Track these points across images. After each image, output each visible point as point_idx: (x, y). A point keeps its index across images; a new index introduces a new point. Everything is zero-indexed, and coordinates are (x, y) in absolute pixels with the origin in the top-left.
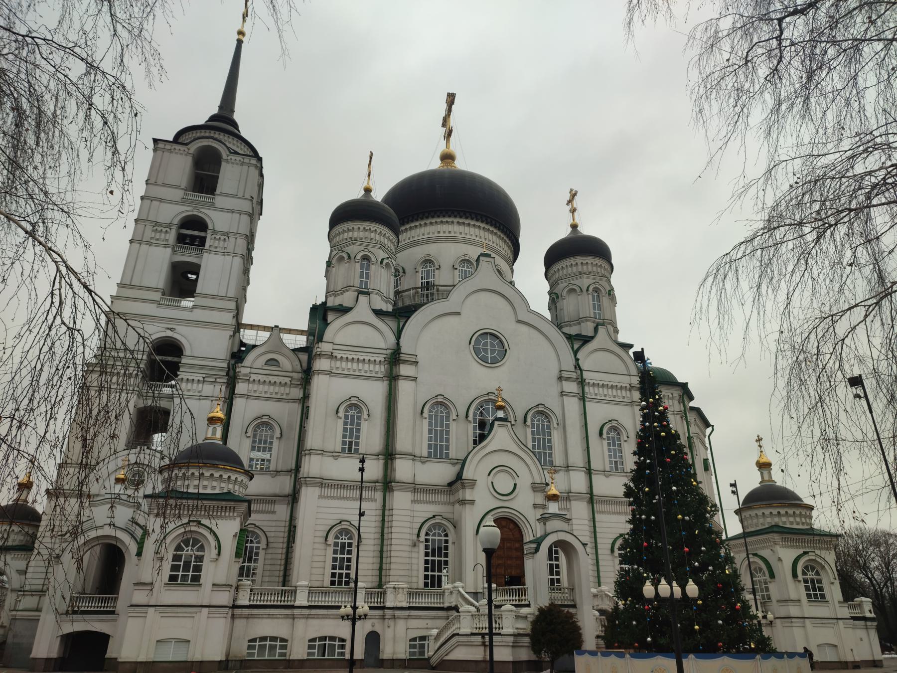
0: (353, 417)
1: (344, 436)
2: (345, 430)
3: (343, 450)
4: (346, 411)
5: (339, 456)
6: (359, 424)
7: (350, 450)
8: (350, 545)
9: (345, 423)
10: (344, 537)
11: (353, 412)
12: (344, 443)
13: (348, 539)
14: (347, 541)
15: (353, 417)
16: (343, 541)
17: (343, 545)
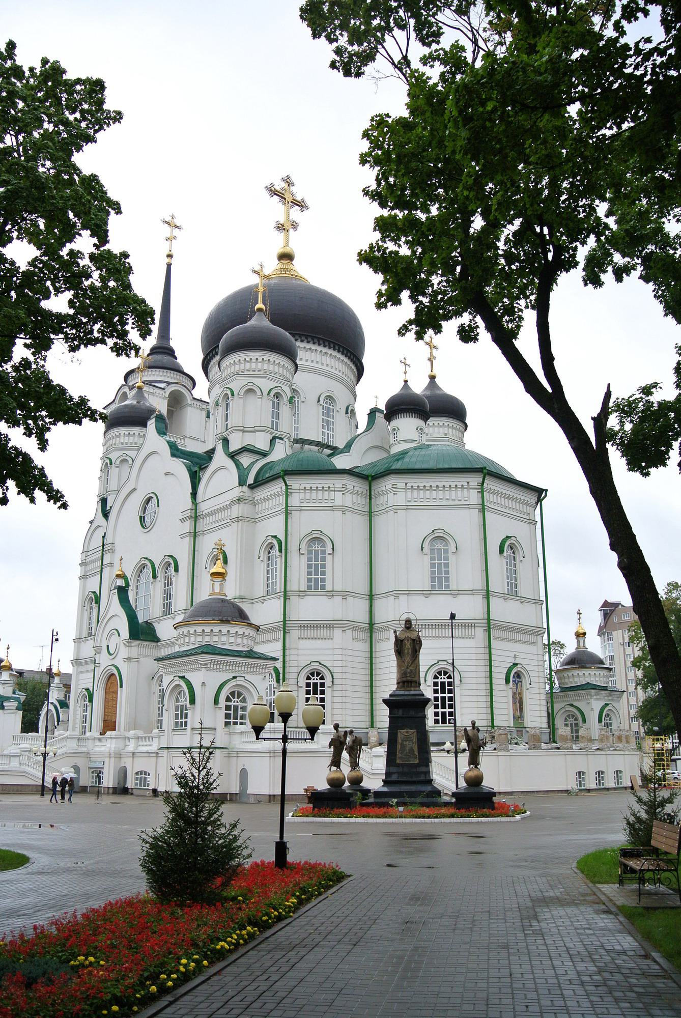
0: (316, 552)
1: (309, 573)
2: (309, 566)
3: (309, 587)
4: (309, 546)
5: (306, 595)
6: (324, 559)
7: (316, 588)
8: (322, 685)
9: (309, 559)
10: (315, 677)
11: (317, 547)
12: (309, 580)
13: (320, 679)
14: (319, 681)
15: (316, 552)
16: (315, 681)
17: (315, 685)
